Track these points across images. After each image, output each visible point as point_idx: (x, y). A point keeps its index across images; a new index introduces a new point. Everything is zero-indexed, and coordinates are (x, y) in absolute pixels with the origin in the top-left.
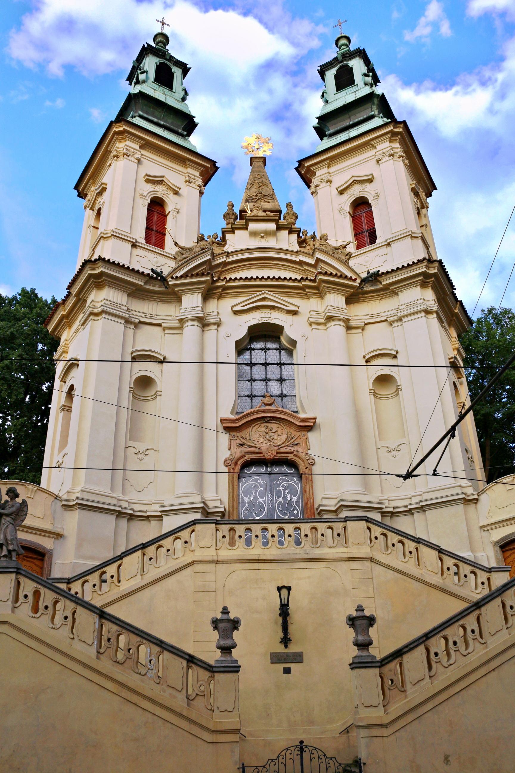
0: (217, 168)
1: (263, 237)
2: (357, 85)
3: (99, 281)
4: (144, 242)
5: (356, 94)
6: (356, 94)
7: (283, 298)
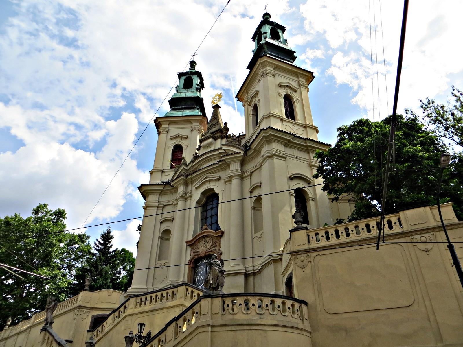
0: (314, 77)
3: (268, 140)
4: (286, 118)
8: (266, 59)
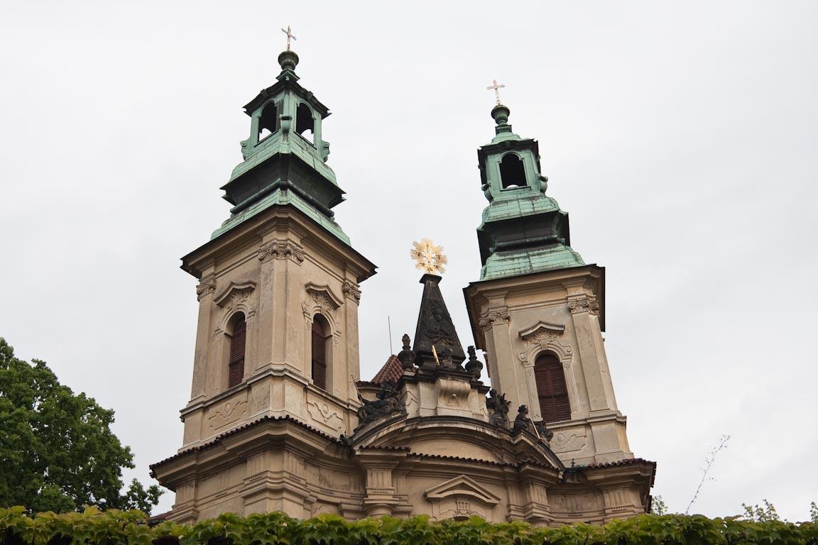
1: (453, 398)
2: (530, 187)
4: (312, 382)
5: (533, 204)
6: (533, 204)
7: (478, 483)
8: (290, 215)
